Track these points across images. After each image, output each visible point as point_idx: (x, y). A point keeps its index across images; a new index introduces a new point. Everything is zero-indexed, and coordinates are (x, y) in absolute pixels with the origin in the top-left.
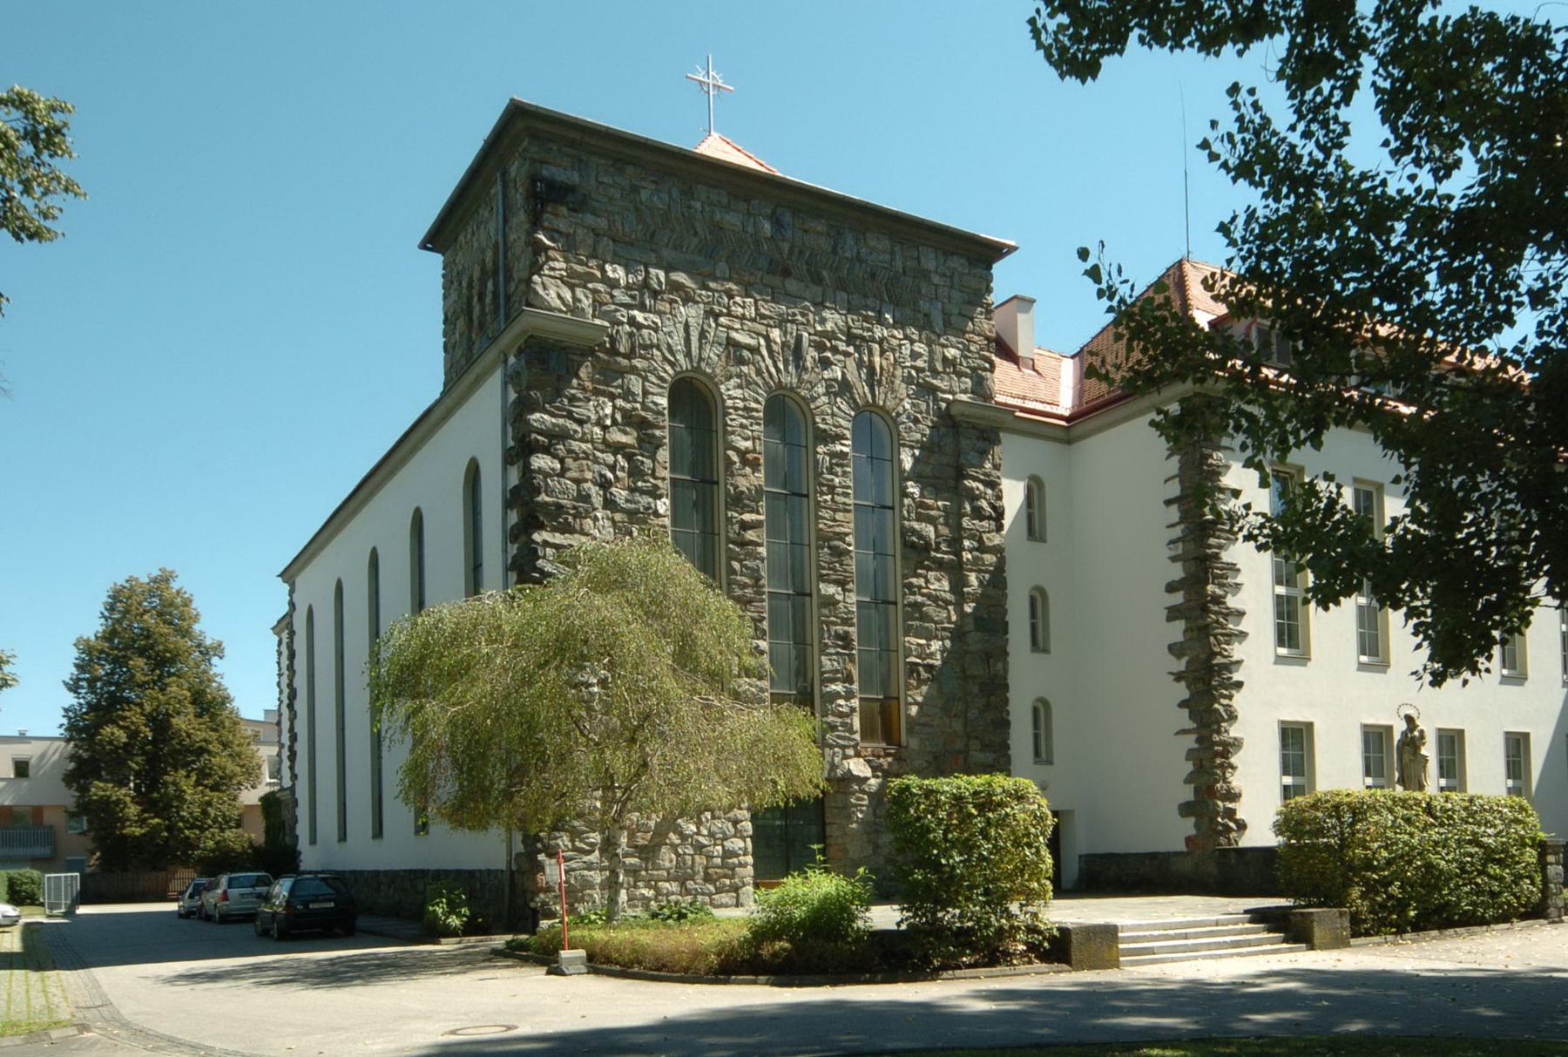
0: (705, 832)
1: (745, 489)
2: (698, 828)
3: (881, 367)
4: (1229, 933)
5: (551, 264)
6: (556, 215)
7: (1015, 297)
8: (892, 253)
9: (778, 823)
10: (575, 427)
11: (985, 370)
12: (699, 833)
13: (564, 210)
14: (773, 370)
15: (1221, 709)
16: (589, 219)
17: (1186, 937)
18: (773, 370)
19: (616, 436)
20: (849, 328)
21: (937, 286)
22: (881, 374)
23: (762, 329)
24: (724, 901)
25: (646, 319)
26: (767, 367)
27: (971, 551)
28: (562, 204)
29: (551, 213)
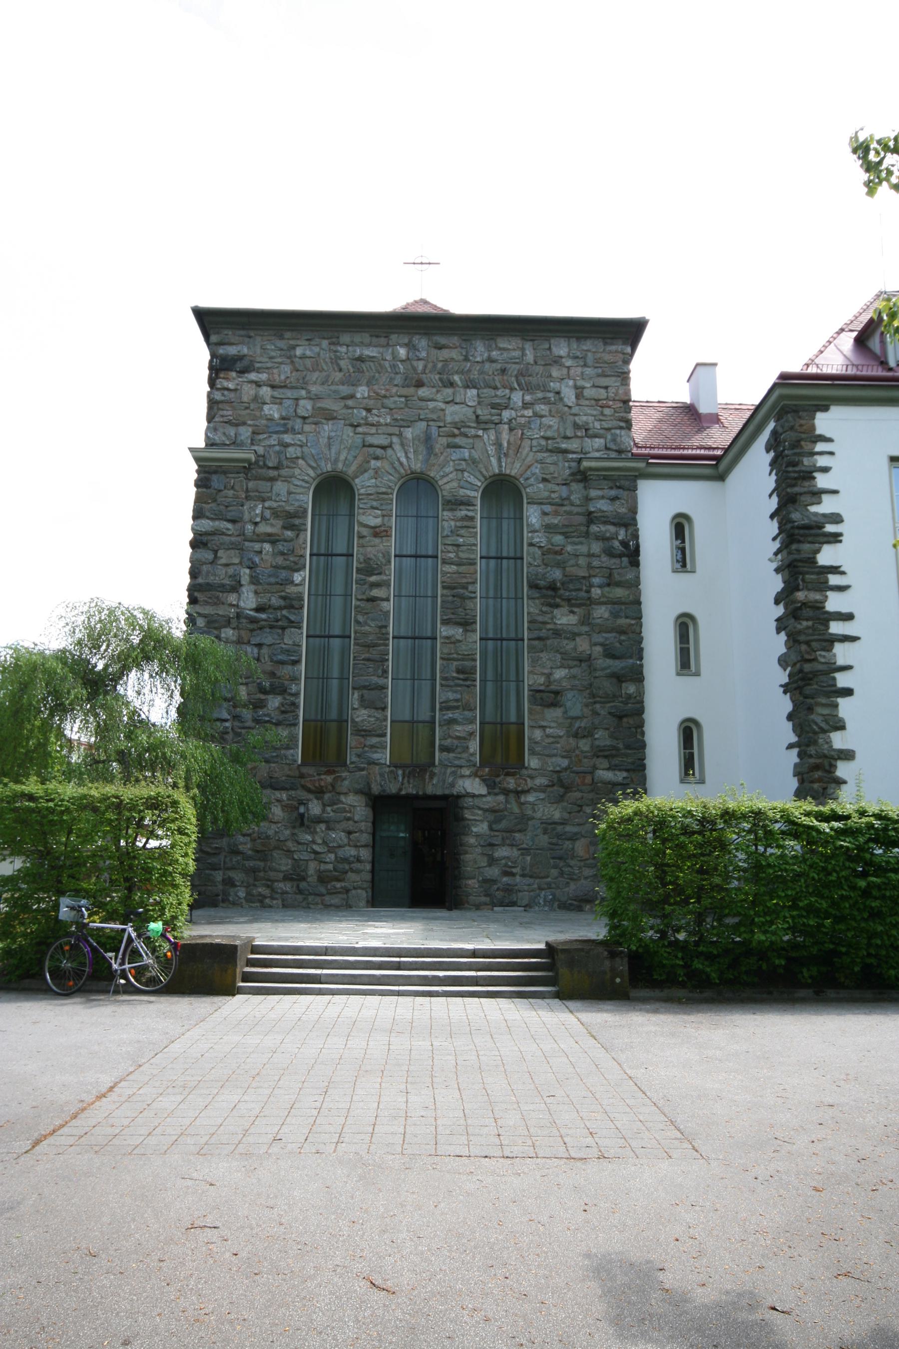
0: (320, 841)
1: (372, 556)
2: (313, 837)
3: (509, 443)
4: (468, 966)
5: (221, 413)
6: (227, 379)
7: (698, 365)
8: (523, 349)
9: (402, 835)
10: (230, 526)
11: (621, 428)
12: (314, 842)
13: (234, 374)
14: (404, 460)
15: (819, 719)
16: (253, 376)
17: (398, 966)
18: (404, 460)
19: (263, 528)
20: (477, 417)
21: (568, 368)
22: (508, 448)
23: (396, 430)
24: (332, 902)
25: (293, 440)
26: (398, 460)
27: (600, 587)
28: (232, 370)
29: (224, 378)
